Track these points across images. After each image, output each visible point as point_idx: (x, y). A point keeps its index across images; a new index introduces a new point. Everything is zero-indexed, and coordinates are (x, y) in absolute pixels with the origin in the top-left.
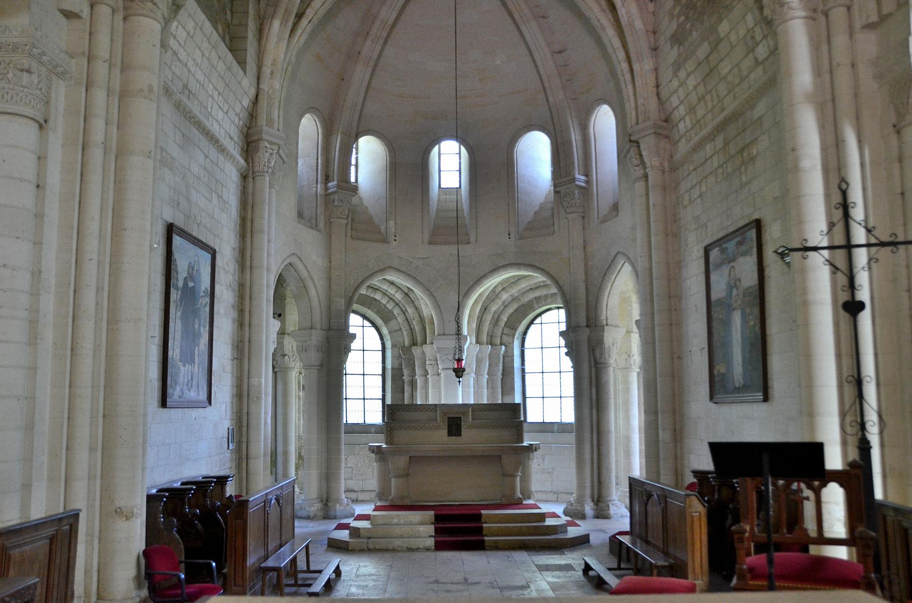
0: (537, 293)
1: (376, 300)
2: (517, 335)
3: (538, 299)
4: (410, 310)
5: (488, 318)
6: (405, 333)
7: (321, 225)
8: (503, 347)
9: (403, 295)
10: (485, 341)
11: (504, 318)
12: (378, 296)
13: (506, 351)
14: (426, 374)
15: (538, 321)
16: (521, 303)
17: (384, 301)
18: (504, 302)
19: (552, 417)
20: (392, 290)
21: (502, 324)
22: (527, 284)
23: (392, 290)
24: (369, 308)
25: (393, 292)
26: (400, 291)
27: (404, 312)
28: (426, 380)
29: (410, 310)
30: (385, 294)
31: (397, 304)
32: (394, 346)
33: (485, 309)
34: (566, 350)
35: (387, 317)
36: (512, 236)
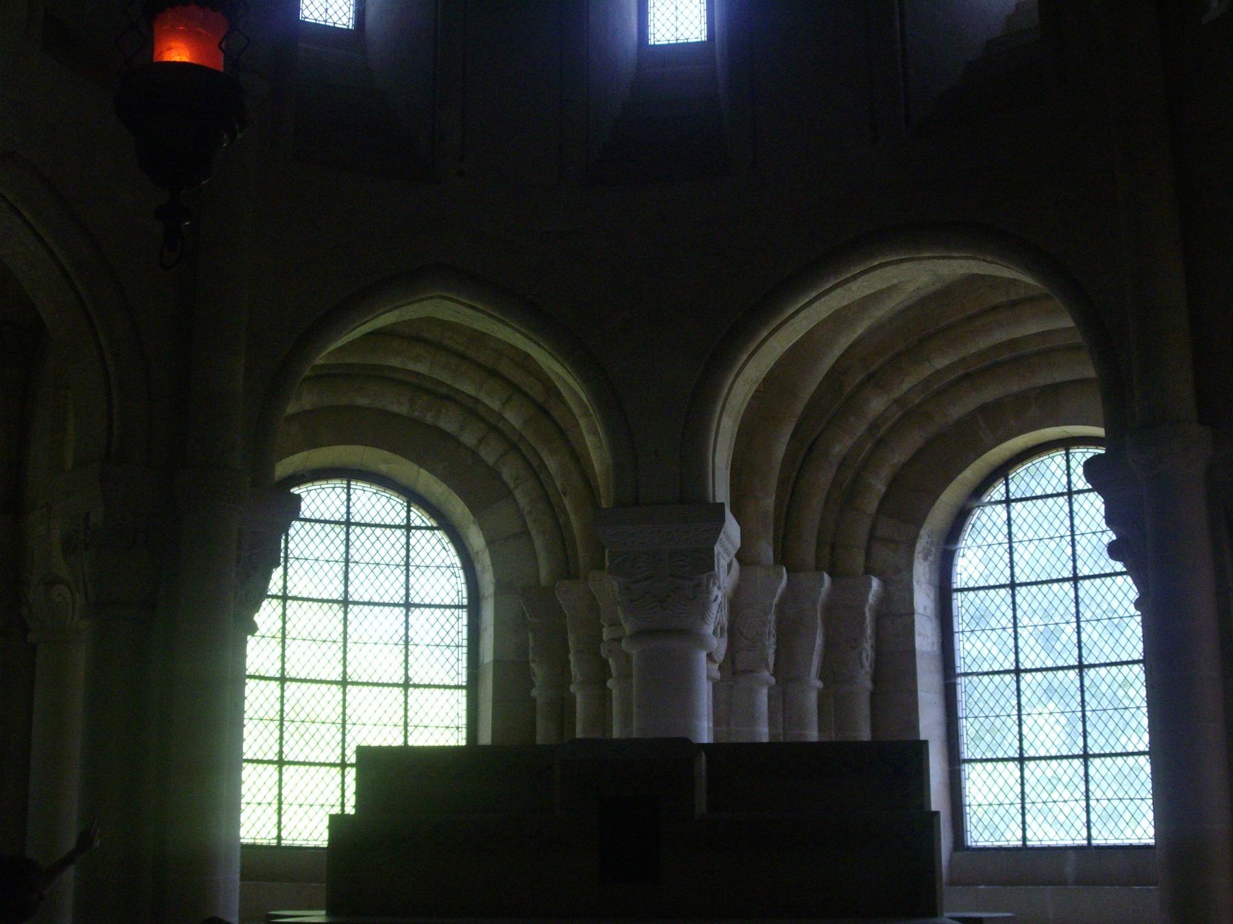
0: (990, 393)
2: (921, 544)
5: (823, 479)
6: (539, 543)
8: (875, 583)
10: (810, 558)
11: (880, 486)
12: (449, 422)
13: (885, 598)
14: (603, 672)
15: (998, 492)
17: (469, 438)
18: (874, 426)
19: (1057, 827)
21: (872, 505)
24: (421, 462)
25: (495, 405)
27: (536, 472)
28: (605, 696)
30: (471, 410)
32: (502, 587)
33: (806, 451)
34: (1111, 536)
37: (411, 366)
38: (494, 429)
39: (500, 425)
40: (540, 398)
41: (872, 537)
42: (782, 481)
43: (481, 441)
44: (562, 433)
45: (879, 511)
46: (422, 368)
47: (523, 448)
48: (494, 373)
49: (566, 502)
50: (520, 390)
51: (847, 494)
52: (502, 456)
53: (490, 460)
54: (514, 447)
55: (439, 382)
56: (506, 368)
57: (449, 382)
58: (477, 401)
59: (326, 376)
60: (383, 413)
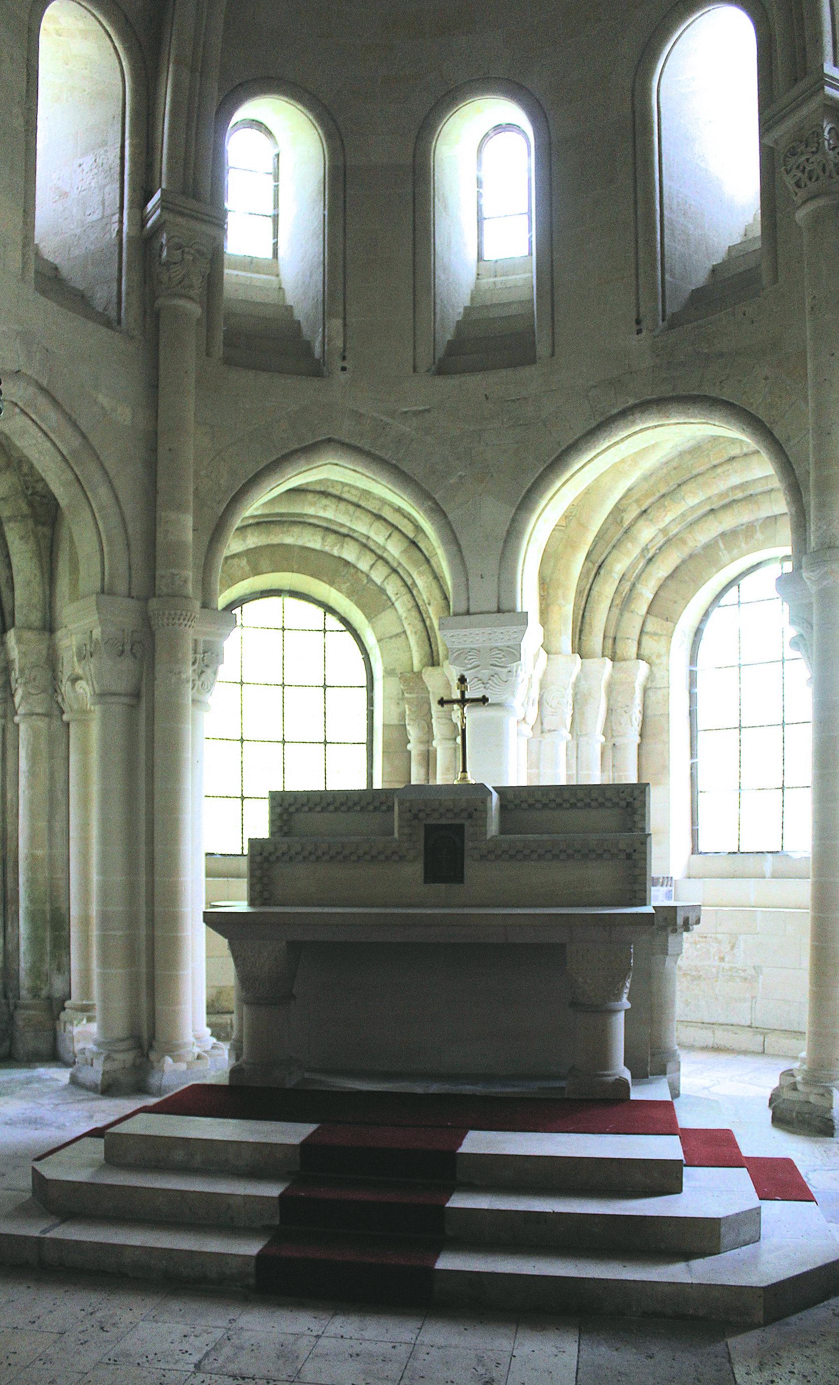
1: (347, 563)
3: (729, 537)
4: (422, 582)
5: (607, 590)
7: (130, 316)
9: (406, 544)
12: (349, 553)
16: (686, 551)
17: (363, 565)
20: (378, 535)
22: (701, 496)
23: (378, 535)
24: (331, 583)
25: (381, 540)
26: (396, 536)
27: (410, 589)
29: (422, 582)
30: (365, 546)
31: (395, 571)
33: (596, 568)
35: (373, 601)
36: (644, 325)
37: (321, 513)
38: (380, 557)
39: (385, 555)
40: (411, 535)
41: (642, 632)
42: (579, 593)
43: (372, 566)
44: (428, 561)
45: (648, 613)
46: (329, 514)
47: (399, 570)
48: (379, 517)
49: (431, 609)
50: (396, 528)
51: (624, 601)
52: (386, 578)
53: (379, 581)
54: (395, 571)
55: (342, 525)
56: (387, 513)
57: (348, 524)
58: (368, 538)
59: (263, 523)
60: (304, 548)
